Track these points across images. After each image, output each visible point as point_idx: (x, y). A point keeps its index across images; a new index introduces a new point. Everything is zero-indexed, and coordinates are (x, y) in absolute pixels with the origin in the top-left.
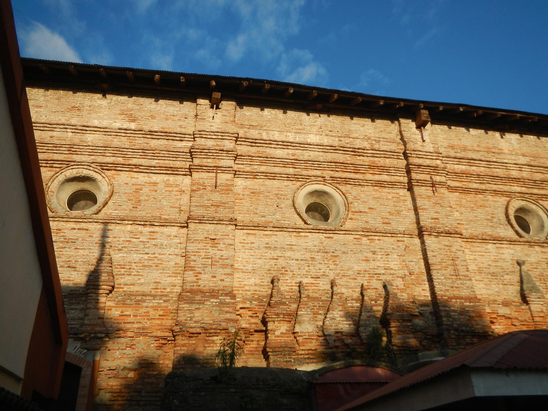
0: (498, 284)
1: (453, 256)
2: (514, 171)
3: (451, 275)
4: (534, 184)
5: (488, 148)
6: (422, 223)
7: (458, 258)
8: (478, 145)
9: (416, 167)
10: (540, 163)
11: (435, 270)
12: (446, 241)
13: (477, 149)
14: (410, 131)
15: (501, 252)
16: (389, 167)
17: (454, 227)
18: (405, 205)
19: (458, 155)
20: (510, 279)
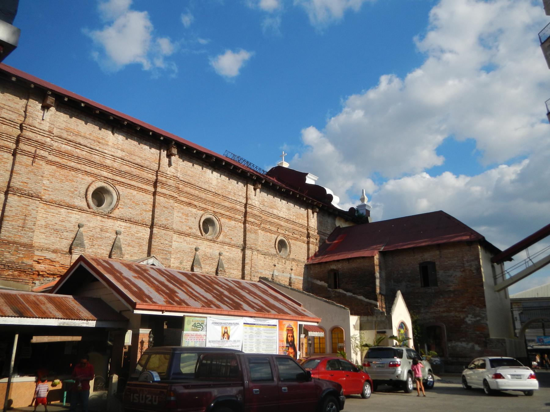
0: (56, 237)
1: (27, 213)
2: (109, 160)
3: (18, 226)
4: (119, 173)
5: (98, 138)
6: (11, 184)
7: (31, 215)
8: (91, 134)
9: (26, 139)
10: (131, 159)
11: (7, 221)
12: (25, 201)
13: (88, 136)
14: (35, 107)
15: (69, 216)
16: (2, 133)
17: (38, 192)
18: (4, 166)
19: (69, 138)
20: (67, 235)
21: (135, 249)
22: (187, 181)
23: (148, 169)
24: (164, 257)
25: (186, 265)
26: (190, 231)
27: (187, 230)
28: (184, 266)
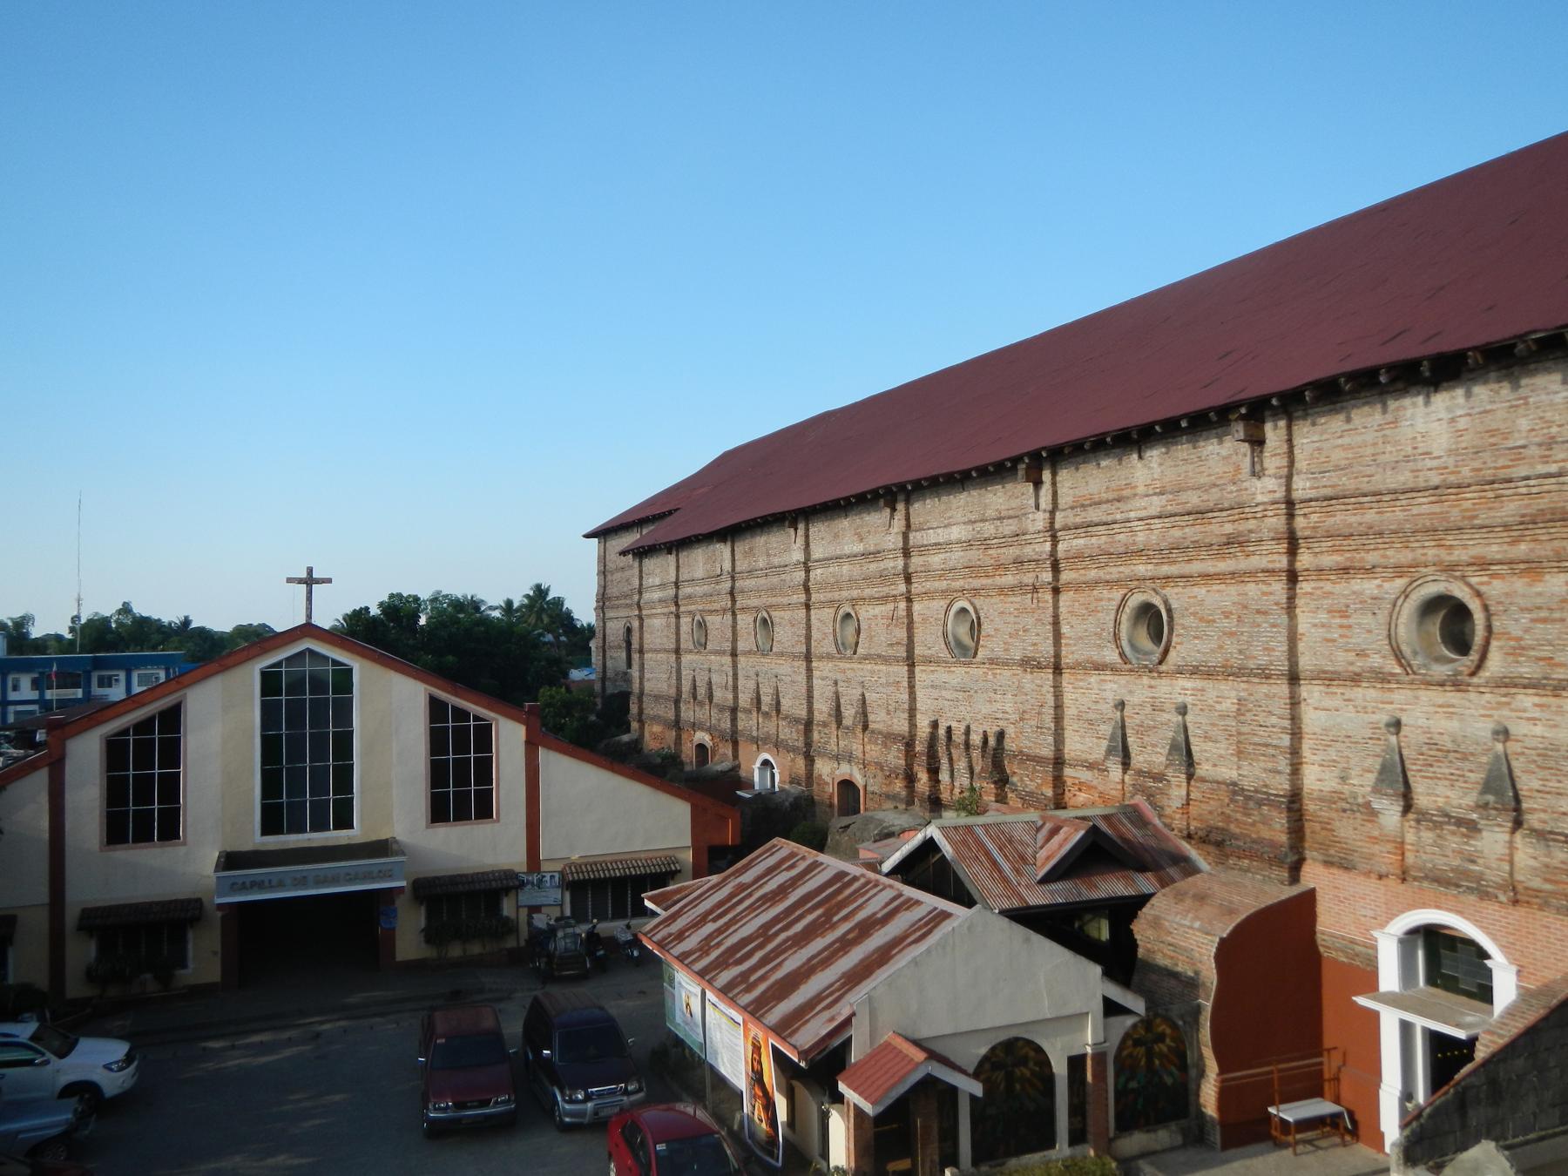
21: (1218, 745)
22: (1328, 492)
23: (1215, 514)
24: (1270, 765)
25: (1362, 786)
26: (1359, 665)
27: (1352, 664)
28: (1355, 789)
